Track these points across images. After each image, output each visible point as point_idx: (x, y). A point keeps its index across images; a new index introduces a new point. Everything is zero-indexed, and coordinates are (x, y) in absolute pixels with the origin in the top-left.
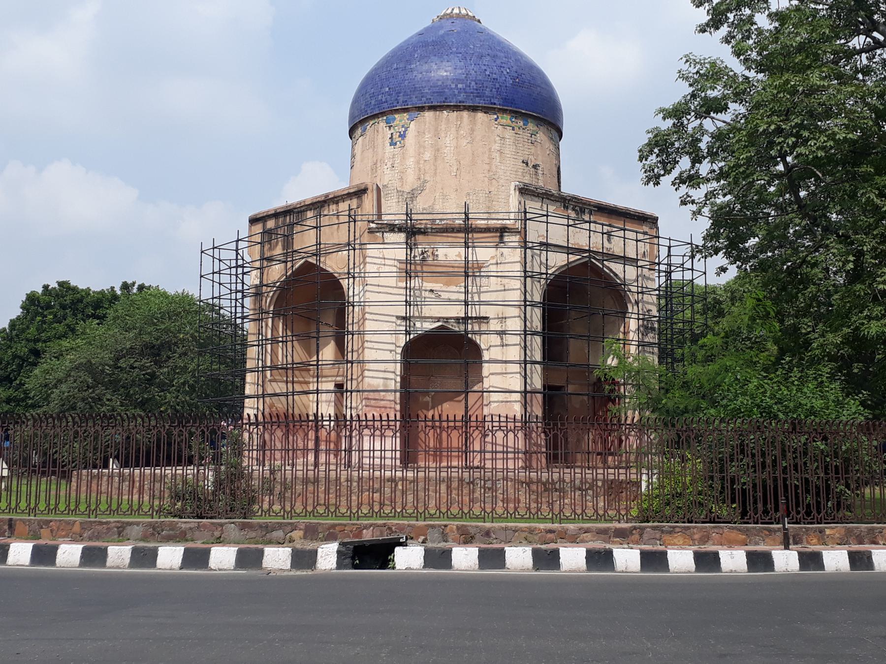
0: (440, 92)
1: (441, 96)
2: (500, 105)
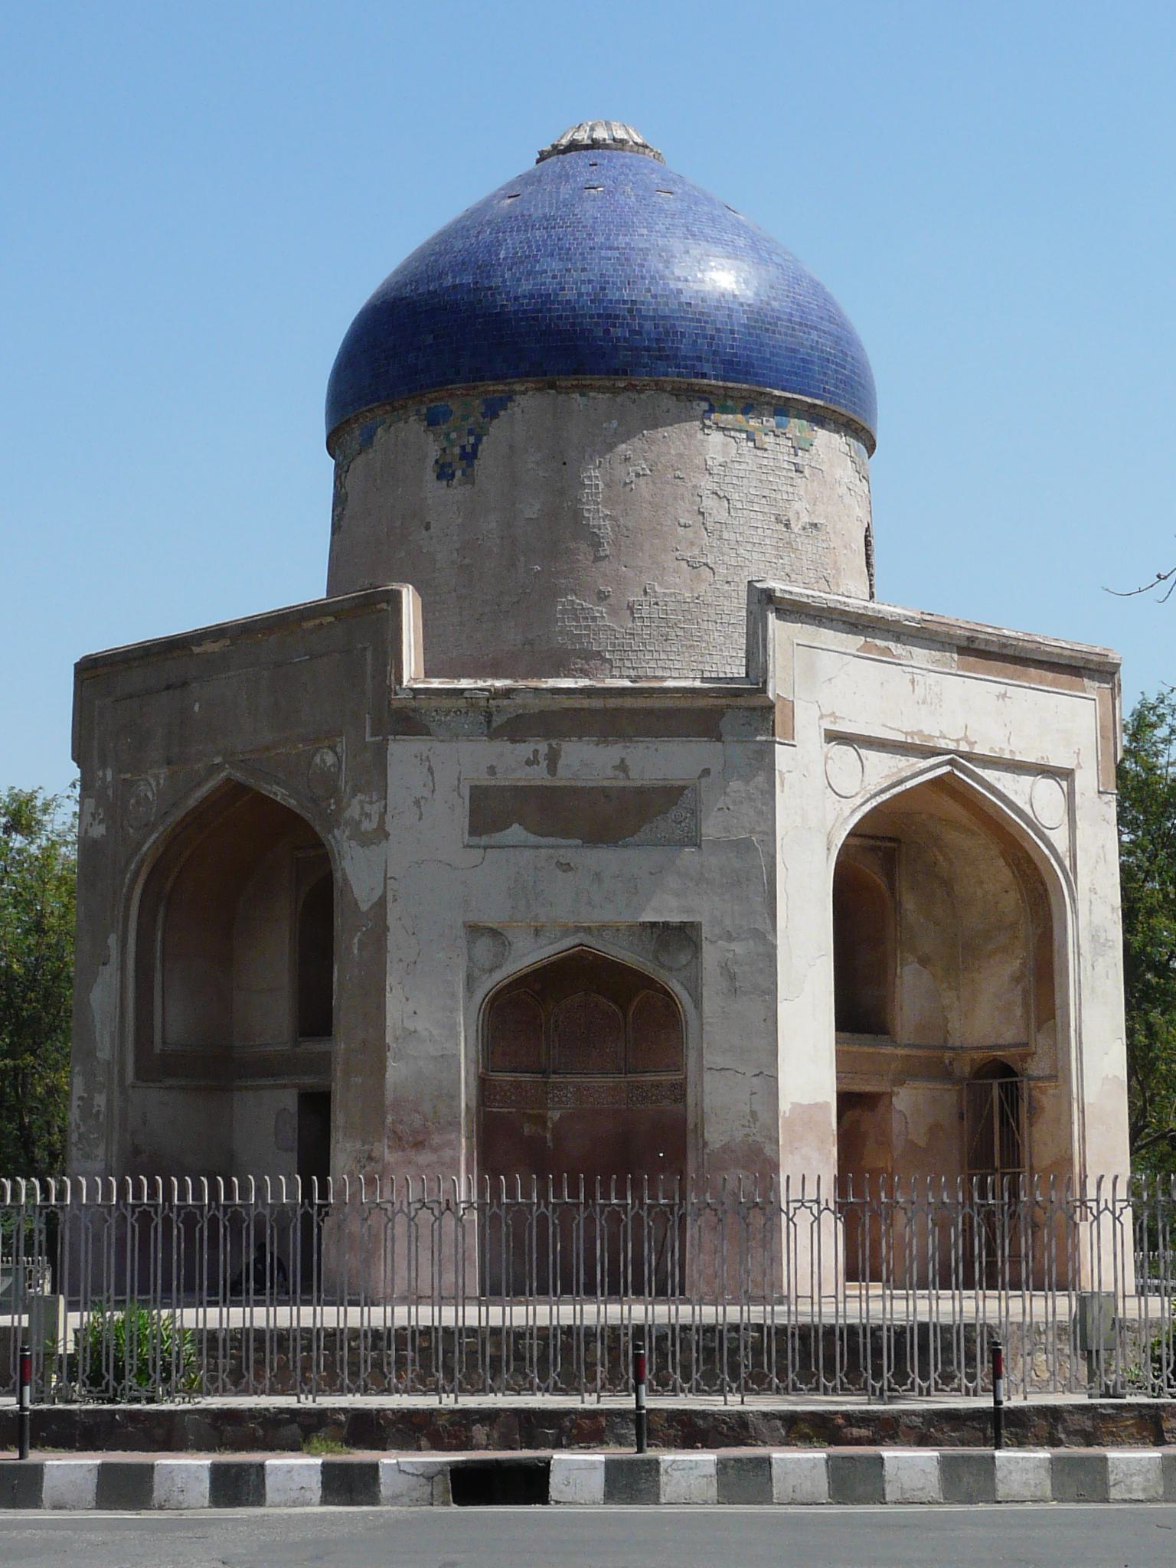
2: (716, 378)
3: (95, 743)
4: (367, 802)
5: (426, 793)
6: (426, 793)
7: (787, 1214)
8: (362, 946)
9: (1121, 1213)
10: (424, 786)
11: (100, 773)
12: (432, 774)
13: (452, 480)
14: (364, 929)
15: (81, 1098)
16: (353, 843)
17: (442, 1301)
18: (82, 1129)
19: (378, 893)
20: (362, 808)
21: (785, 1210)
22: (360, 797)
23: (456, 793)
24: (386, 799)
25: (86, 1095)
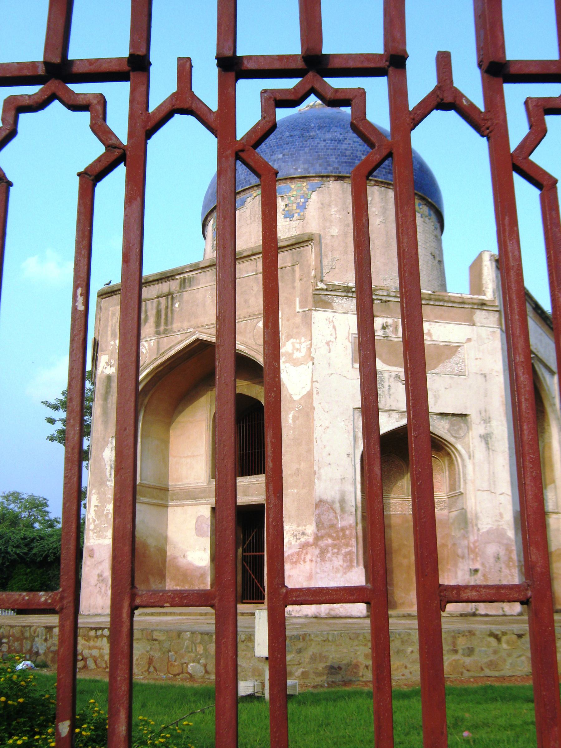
0: (350, 163)
1: (351, 166)
3: (109, 328)
4: (297, 343)
5: (333, 340)
6: (333, 340)
8: (295, 418)
10: (331, 335)
11: (112, 343)
12: (335, 330)
13: (293, 217)
14: (297, 409)
15: (95, 506)
18: (97, 522)
19: (308, 388)
20: (294, 346)
22: (292, 340)
23: (347, 340)
24: (311, 340)
25: (99, 505)
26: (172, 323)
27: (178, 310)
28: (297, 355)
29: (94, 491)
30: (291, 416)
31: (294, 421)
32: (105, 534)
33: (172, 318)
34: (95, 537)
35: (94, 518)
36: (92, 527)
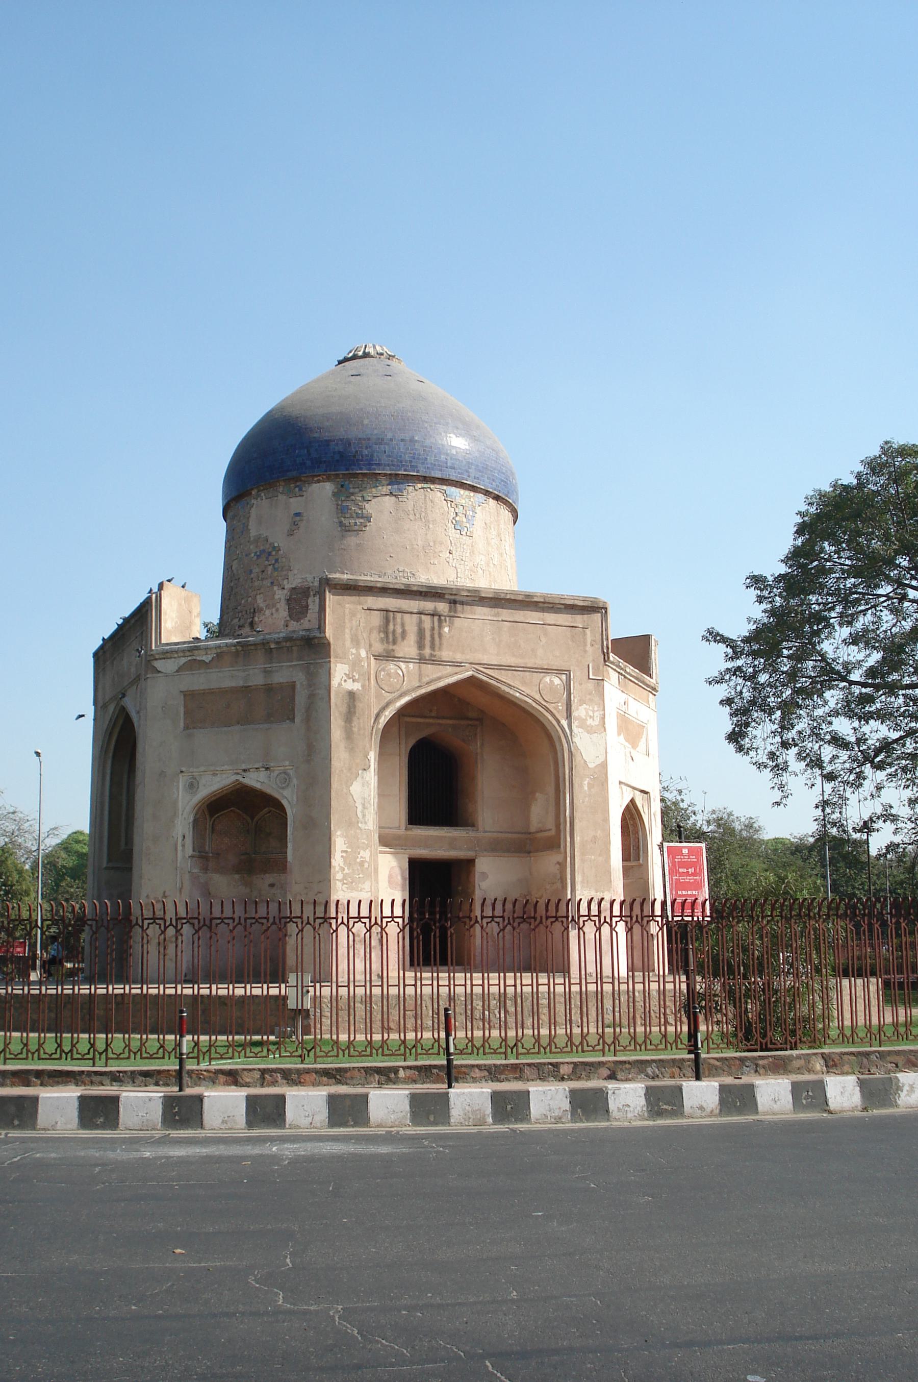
3: (347, 631)
7: (142, 927)
8: (590, 786)
9: (584, 924)
11: (354, 651)
15: (342, 851)
16: (580, 730)
17: (193, 982)
20: (587, 713)
21: (175, 925)
25: (349, 850)
26: (440, 649)
27: (448, 636)
28: (589, 722)
29: (339, 833)
30: (586, 782)
31: (589, 788)
32: (360, 885)
33: (440, 644)
34: (345, 889)
35: (342, 865)
36: (339, 876)
